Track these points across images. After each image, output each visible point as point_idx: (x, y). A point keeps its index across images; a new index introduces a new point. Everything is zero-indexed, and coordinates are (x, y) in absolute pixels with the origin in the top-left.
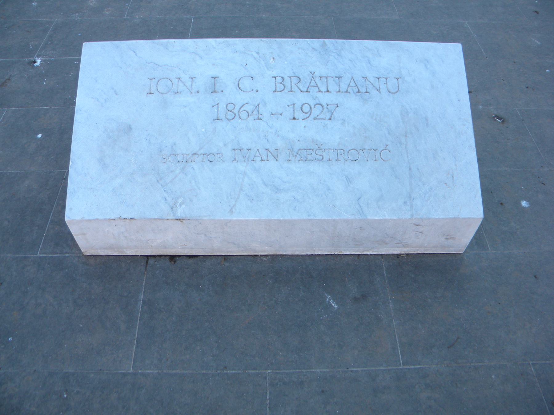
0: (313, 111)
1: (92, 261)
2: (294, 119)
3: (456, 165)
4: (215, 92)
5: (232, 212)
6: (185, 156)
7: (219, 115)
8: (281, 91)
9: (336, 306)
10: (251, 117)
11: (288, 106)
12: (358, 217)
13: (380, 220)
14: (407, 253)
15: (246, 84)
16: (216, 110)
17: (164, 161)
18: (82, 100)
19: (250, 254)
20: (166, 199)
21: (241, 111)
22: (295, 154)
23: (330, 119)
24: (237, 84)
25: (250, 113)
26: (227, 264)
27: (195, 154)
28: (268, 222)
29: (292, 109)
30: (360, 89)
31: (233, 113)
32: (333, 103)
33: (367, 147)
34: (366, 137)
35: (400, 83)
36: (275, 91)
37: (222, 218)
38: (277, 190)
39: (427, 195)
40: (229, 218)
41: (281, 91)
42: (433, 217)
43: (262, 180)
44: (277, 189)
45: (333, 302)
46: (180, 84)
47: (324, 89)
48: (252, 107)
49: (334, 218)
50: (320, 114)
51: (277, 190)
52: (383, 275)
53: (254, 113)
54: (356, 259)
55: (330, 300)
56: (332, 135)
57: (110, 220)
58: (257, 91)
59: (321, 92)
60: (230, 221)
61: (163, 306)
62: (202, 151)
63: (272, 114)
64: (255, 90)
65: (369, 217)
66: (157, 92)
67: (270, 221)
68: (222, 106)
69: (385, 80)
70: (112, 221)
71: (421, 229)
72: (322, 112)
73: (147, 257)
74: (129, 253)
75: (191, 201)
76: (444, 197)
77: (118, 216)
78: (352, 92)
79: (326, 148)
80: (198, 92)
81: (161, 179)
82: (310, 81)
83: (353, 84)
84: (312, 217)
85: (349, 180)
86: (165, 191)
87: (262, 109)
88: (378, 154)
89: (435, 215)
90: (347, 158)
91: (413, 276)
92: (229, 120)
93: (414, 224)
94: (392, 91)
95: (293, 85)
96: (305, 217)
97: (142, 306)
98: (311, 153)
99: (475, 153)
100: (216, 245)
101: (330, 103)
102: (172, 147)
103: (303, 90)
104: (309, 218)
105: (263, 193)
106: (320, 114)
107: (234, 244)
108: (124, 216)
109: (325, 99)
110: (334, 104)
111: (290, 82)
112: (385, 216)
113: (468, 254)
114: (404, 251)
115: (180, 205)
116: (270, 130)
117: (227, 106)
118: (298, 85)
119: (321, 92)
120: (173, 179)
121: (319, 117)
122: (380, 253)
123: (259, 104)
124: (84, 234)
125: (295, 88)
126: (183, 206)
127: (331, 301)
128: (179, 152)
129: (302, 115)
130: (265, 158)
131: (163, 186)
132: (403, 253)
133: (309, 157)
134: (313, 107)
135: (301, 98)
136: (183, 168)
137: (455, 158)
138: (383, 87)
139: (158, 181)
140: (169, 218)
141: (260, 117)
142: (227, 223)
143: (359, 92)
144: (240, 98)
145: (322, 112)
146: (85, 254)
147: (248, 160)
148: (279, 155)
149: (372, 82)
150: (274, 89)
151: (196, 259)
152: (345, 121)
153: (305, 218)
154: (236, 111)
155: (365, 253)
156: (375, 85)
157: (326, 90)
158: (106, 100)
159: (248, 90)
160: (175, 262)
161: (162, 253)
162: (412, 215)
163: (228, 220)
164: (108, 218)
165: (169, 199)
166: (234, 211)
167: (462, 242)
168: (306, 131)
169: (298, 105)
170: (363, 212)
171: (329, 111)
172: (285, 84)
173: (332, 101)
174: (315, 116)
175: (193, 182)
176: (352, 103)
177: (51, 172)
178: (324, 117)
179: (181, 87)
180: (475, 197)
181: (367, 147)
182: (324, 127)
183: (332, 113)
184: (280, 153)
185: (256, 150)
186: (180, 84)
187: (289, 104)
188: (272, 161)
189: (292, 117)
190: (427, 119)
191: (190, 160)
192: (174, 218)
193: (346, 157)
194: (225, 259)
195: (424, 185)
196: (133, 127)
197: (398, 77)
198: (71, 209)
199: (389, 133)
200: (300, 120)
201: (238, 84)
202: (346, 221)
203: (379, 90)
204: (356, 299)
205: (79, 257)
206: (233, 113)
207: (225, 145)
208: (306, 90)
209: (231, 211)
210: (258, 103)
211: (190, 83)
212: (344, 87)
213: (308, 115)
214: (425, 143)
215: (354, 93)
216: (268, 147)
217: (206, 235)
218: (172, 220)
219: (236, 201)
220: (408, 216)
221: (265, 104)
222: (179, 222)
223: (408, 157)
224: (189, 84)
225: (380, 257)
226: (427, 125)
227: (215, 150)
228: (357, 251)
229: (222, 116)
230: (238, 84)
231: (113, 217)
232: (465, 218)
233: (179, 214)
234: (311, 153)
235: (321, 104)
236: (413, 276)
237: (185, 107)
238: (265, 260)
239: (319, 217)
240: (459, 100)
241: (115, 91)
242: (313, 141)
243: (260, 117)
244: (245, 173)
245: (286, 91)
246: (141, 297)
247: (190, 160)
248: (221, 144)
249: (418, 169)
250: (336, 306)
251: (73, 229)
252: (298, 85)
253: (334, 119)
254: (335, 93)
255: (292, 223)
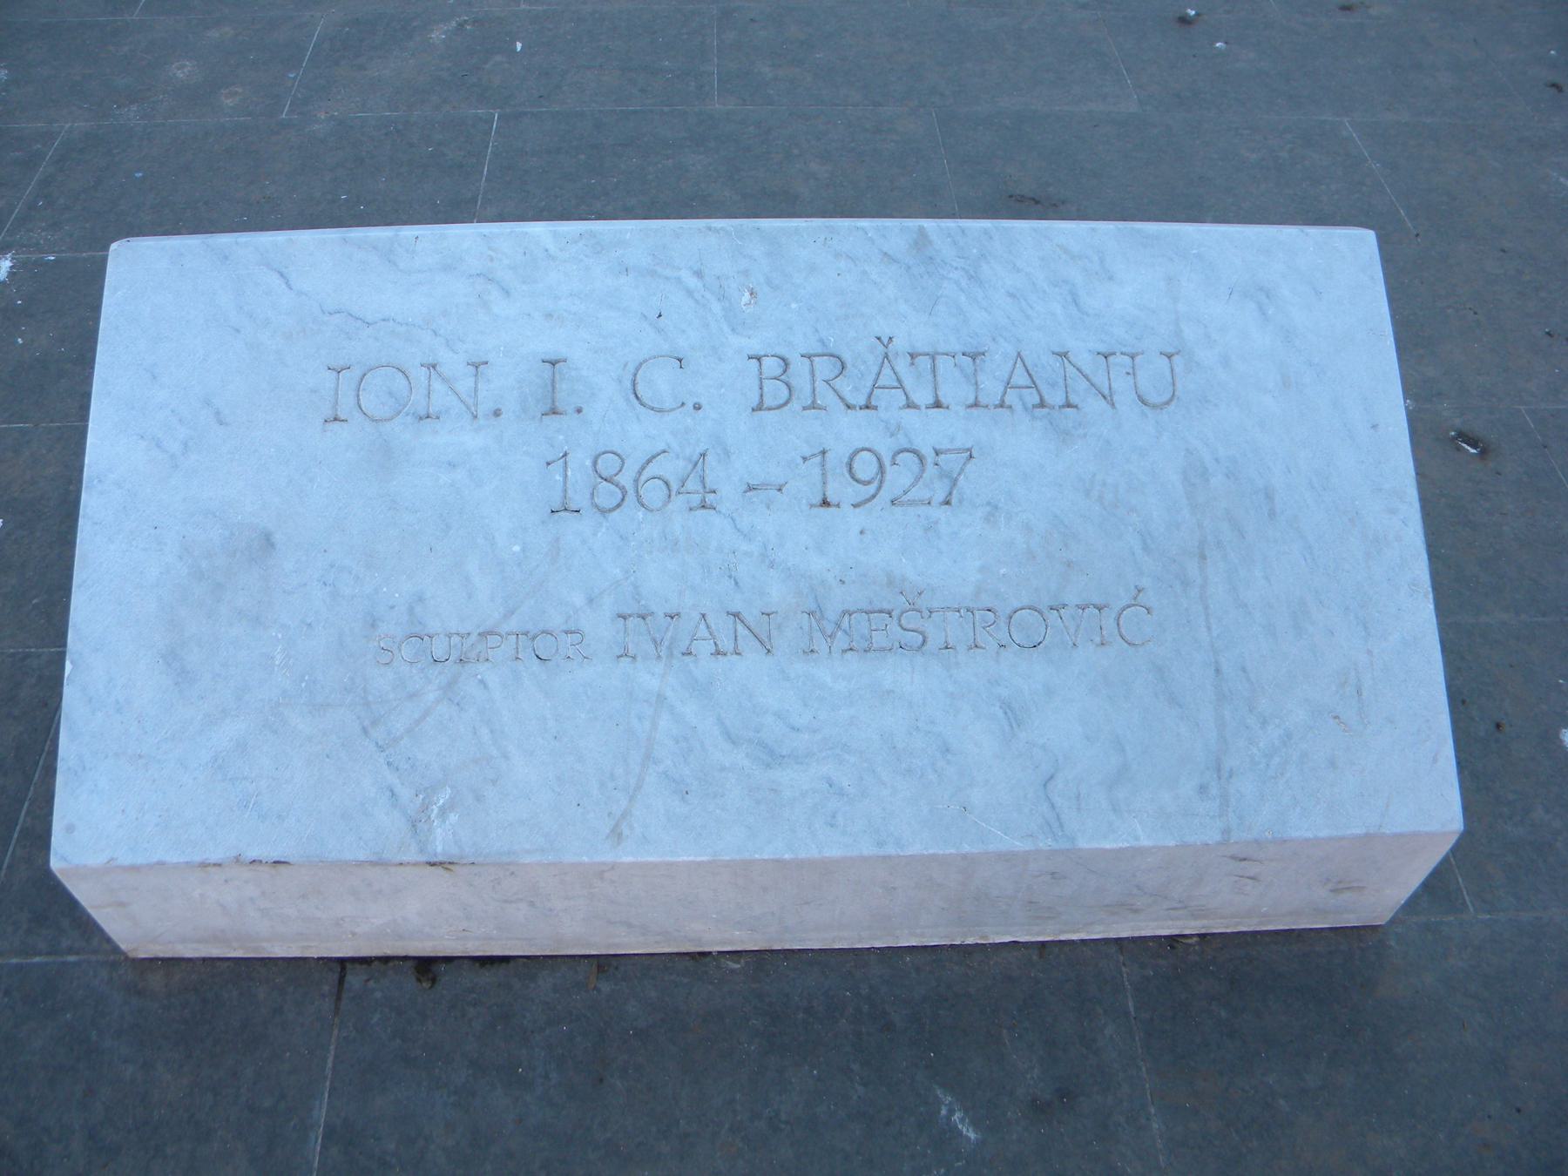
0: (888, 477)
1: (156, 981)
2: (825, 503)
3: (1369, 652)
4: (554, 412)
5: (620, 835)
6: (455, 640)
7: (570, 493)
8: (779, 407)
9: (972, 1135)
10: (678, 502)
11: (805, 459)
12: (1045, 843)
13: (1120, 850)
14: (1203, 931)
15: (660, 382)
16: (559, 478)
17: (385, 658)
18: (108, 446)
19: (683, 950)
20: (393, 794)
21: (643, 478)
22: (829, 629)
23: (947, 503)
24: (628, 384)
25: (674, 486)
26: (606, 987)
27: (491, 633)
28: (743, 869)
29: (817, 471)
30: (1044, 393)
31: (615, 487)
32: (958, 444)
33: (1072, 598)
34: (1069, 564)
35: (1177, 370)
36: (759, 408)
37: (585, 859)
38: (772, 756)
39: (1276, 760)
40: (608, 857)
41: (779, 407)
42: (1295, 834)
43: (720, 721)
44: (771, 753)
45: (962, 1120)
46: (437, 385)
47: (923, 396)
48: (681, 463)
49: (966, 848)
50: (913, 485)
51: (772, 756)
52: (1127, 1013)
53: (690, 485)
54: (1035, 958)
55: (951, 1112)
56: (956, 558)
57: (204, 865)
58: (697, 407)
59: (916, 407)
60: (613, 867)
61: (392, 1147)
62: (513, 624)
63: (751, 488)
64: (690, 405)
65: (1083, 843)
66: (357, 414)
67: (747, 865)
68: (580, 460)
69: (1127, 359)
70: (212, 870)
71: (1253, 869)
72: (918, 479)
73: (342, 962)
74: (279, 951)
75: (479, 798)
76: (1332, 763)
77: (234, 853)
78: (1018, 407)
79: (935, 605)
80: (497, 413)
81: (374, 723)
82: (875, 369)
83: (1020, 378)
84: (891, 850)
85: (1013, 715)
86: (389, 764)
87: (715, 472)
88: (1109, 622)
89: (1300, 828)
90: (1005, 640)
91: (1223, 1014)
92: (604, 512)
93: (1233, 858)
94: (1154, 398)
95: (819, 384)
96: (867, 848)
97: (323, 1146)
98: (884, 622)
99: (1432, 607)
100: (573, 929)
101: (945, 445)
102: (411, 610)
103: (852, 401)
104: (882, 852)
105: (723, 769)
106: (913, 485)
107: (630, 925)
108: (253, 853)
109: (929, 431)
110: (959, 451)
111: (808, 377)
112: (1137, 838)
113: (1399, 930)
114: (1191, 927)
115: (443, 812)
116: (744, 547)
117: (595, 463)
118: (837, 383)
119: (916, 407)
120: (418, 722)
121: (910, 496)
122: (1112, 935)
123: (703, 455)
124: (122, 904)
125: (826, 397)
126: (453, 818)
127: (957, 1117)
128: (434, 625)
129: (852, 492)
130: (726, 644)
131: (381, 749)
132: (1187, 932)
133: (879, 639)
134: (887, 462)
135: (848, 431)
136: (450, 686)
137: (1366, 628)
138: (1121, 384)
139: (365, 731)
140: (405, 859)
141: (710, 498)
142: (602, 871)
143: (1042, 404)
144: (639, 434)
145: (918, 479)
146: (131, 955)
147: (671, 655)
148: (774, 633)
149: (1087, 371)
150: (755, 401)
151: (502, 970)
152: (996, 507)
153: (865, 852)
154: (626, 479)
155: (1063, 938)
156: (1095, 380)
157: (931, 400)
158: (186, 445)
159: (667, 406)
160: (434, 981)
161: (389, 952)
162: (1226, 831)
163: (604, 864)
164: (197, 858)
165: (405, 793)
166: (626, 832)
167: (1383, 896)
168: (870, 546)
169: (838, 453)
170: (1061, 826)
171: (943, 475)
172: (793, 382)
173: (952, 440)
174: (898, 492)
175: (484, 731)
176: (1020, 443)
177: (27, 656)
178: (926, 494)
179: (441, 397)
180: (1435, 760)
181: (1072, 598)
182: (927, 530)
183: (954, 482)
184: (779, 627)
185: (696, 616)
186: (437, 385)
187: (807, 452)
188: (752, 654)
189: (818, 499)
190: (1269, 495)
191: (473, 655)
192: (424, 859)
193: (1003, 636)
194: (600, 969)
195: (1264, 723)
196: (278, 537)
197: (1170, 350)
198: (70, 829)
199: (1146, 548)
200: (846, 508)
201: (634, 384)
202: (1007, 858)
203: (1108, 398)
204: (1038, 1108)
205: (114, 965)
206: (615, 487)
207: (591, 601)
208: (863, 402)
209: (616, 835)
210: (700, 450)
211: (470, 382)
212: (991, 388)
213: (872, 489)
214: (1267, 578)
215: (1026, 409)
216: (737, 606)
217: (532, 904)
218: (416, 864)
219: (632, 799)
220: (1213, 836)
221: (727, 453)
222: (439, 871)
223: (1209, 629)
224: (465, 385)
225: (1113, 949)
226: (1272, 514)
227: (556, 621)
228: (1038, 934)
229: (579, 499)
230: (634, 384)
231: (214, 858)
232: (1401, 835)
233: (440, 846)
234: (884, 622)
235: (915, 452)
236: (1223, 1014)
237: (452, 465)
238: (733, 971)
239: (915, 849)
240: (1374, 427)
241: (218, 413)
242: (890, 583)
243: (710, 498)
244: (661, 698)
245: (795, 405)
246: (321, 1113)
247: (473, 655)
248: (578, 599)
249: (1244, 670)
250: (972, 1135)
251: (82, 893)
252: (837, 383)
253: (961, 501)
254: (962, 411)
255: (825, 869)
